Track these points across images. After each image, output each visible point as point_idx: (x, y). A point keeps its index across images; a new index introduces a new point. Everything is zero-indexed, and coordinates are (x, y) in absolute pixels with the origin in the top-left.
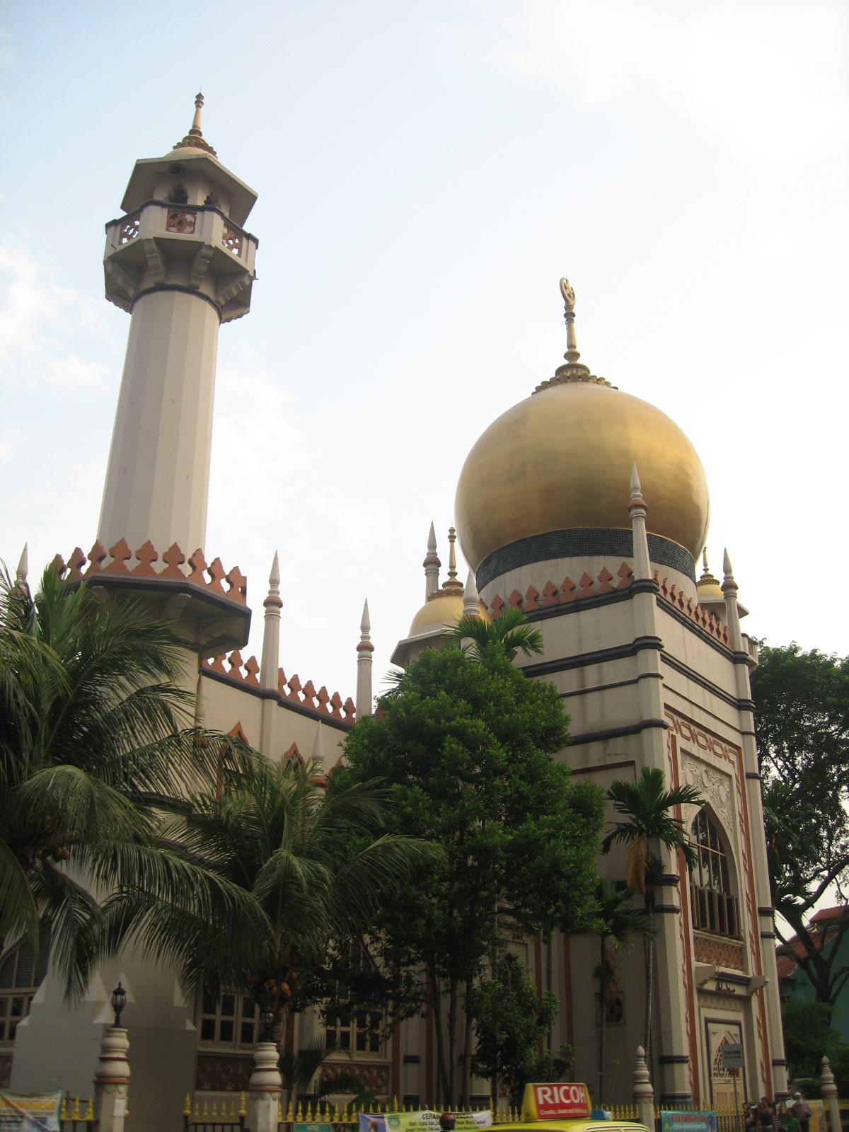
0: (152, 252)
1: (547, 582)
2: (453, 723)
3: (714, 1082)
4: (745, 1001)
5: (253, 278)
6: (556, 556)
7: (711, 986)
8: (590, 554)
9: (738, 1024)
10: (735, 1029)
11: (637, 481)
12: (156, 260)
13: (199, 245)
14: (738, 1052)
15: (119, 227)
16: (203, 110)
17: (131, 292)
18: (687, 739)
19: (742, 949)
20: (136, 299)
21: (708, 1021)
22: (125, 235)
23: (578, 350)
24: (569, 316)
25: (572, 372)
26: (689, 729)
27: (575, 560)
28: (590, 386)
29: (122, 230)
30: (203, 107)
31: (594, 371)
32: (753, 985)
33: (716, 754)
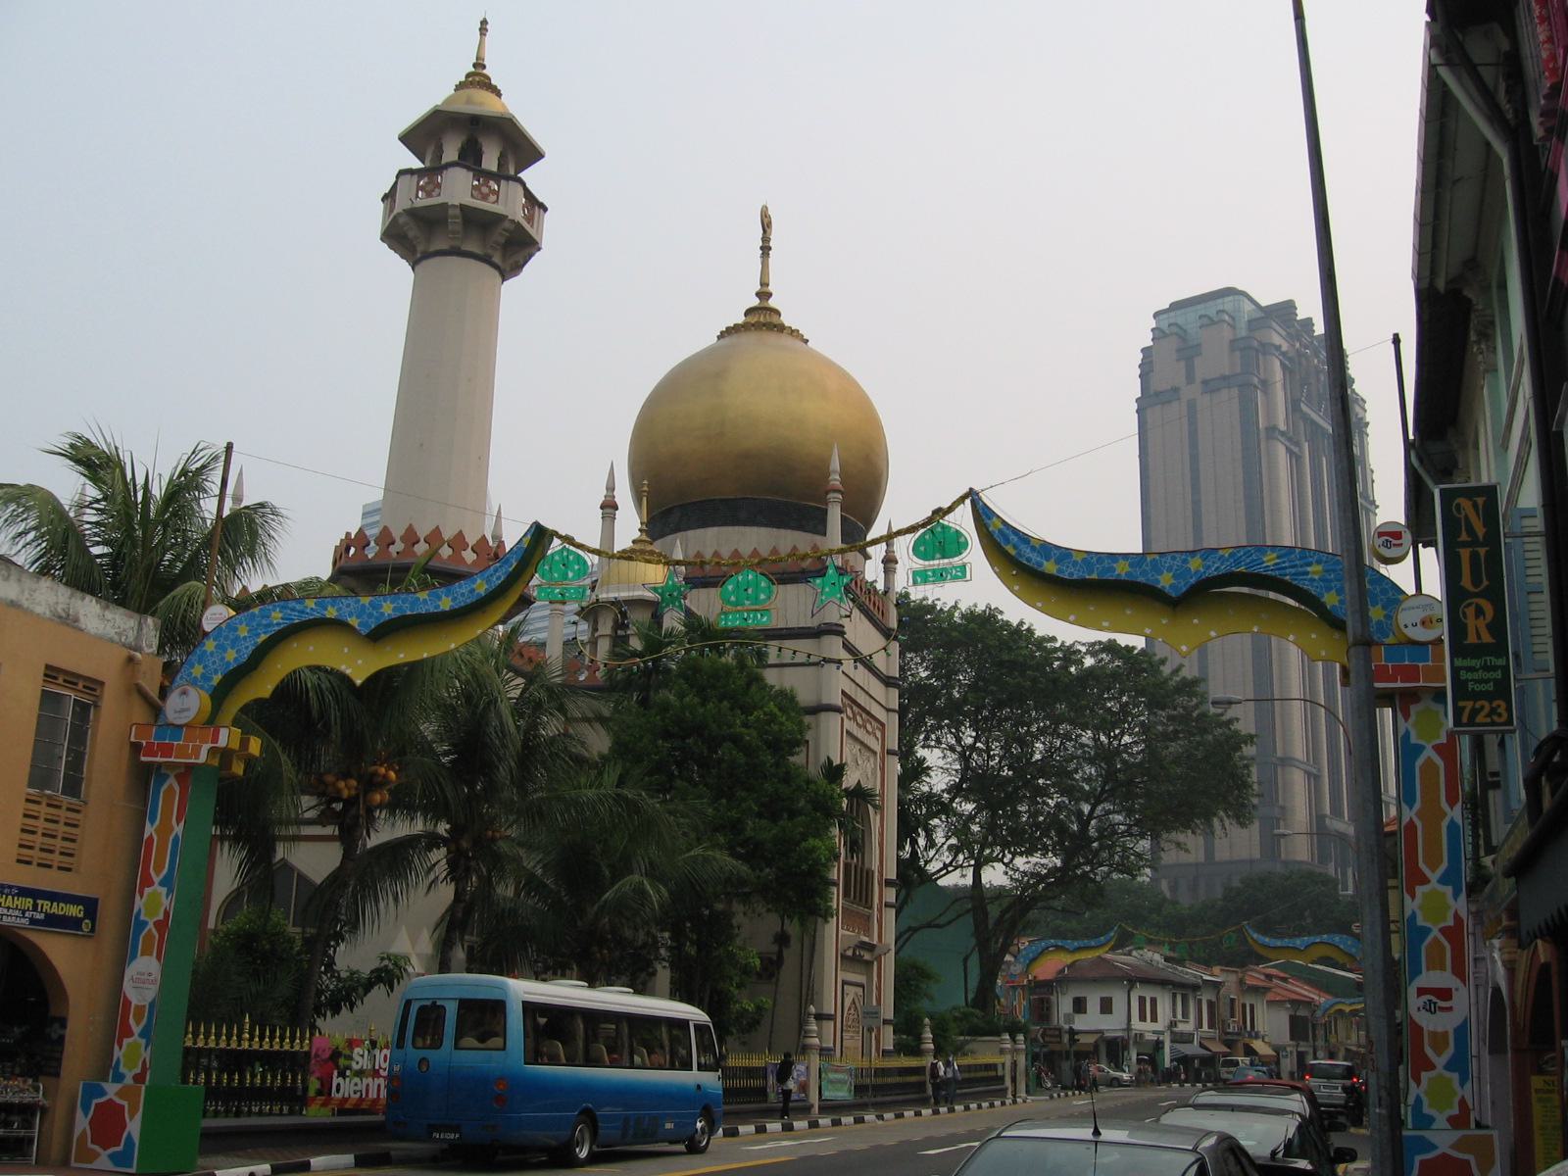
0: (455, 217)
1: (733, 549)
2: (732, 730)
3: (844, 1037)
4: (869, 964)
5: (539, 249)
6: (745, 523)
7: (850, 953)
8: (779, 527)
9: (862, 986)
10: (860, 990)
11: (835, 465)
12: (455, 223)
13: (501, 218)
14: (876, 1013)
15: (415, 177)
16: (487, 39)
17: (420, 248)
18: (850, 719)
19: (869, 918)
20: (427, 256)
21: (844, 983)
22: (419, 188)
23: (771, 288)
24: (766, 249)
25: (762, 319)
26: (852, 709)
27: (763, 530)
28: (785, 340)
29: (418, 183)
30: (488, 34)
31: (787, 320)
32: (877, 952)
33: (867, 731)
